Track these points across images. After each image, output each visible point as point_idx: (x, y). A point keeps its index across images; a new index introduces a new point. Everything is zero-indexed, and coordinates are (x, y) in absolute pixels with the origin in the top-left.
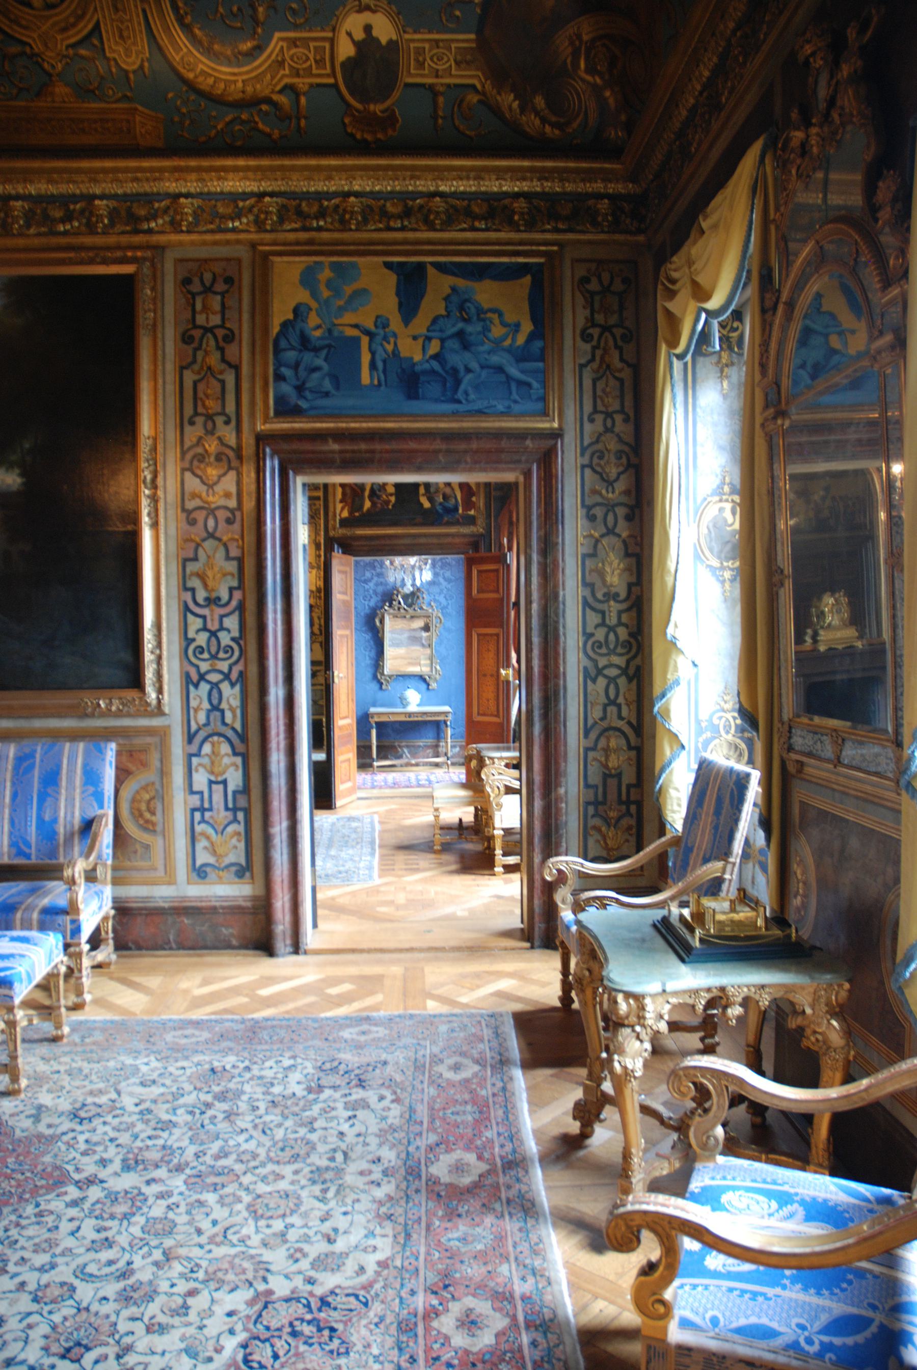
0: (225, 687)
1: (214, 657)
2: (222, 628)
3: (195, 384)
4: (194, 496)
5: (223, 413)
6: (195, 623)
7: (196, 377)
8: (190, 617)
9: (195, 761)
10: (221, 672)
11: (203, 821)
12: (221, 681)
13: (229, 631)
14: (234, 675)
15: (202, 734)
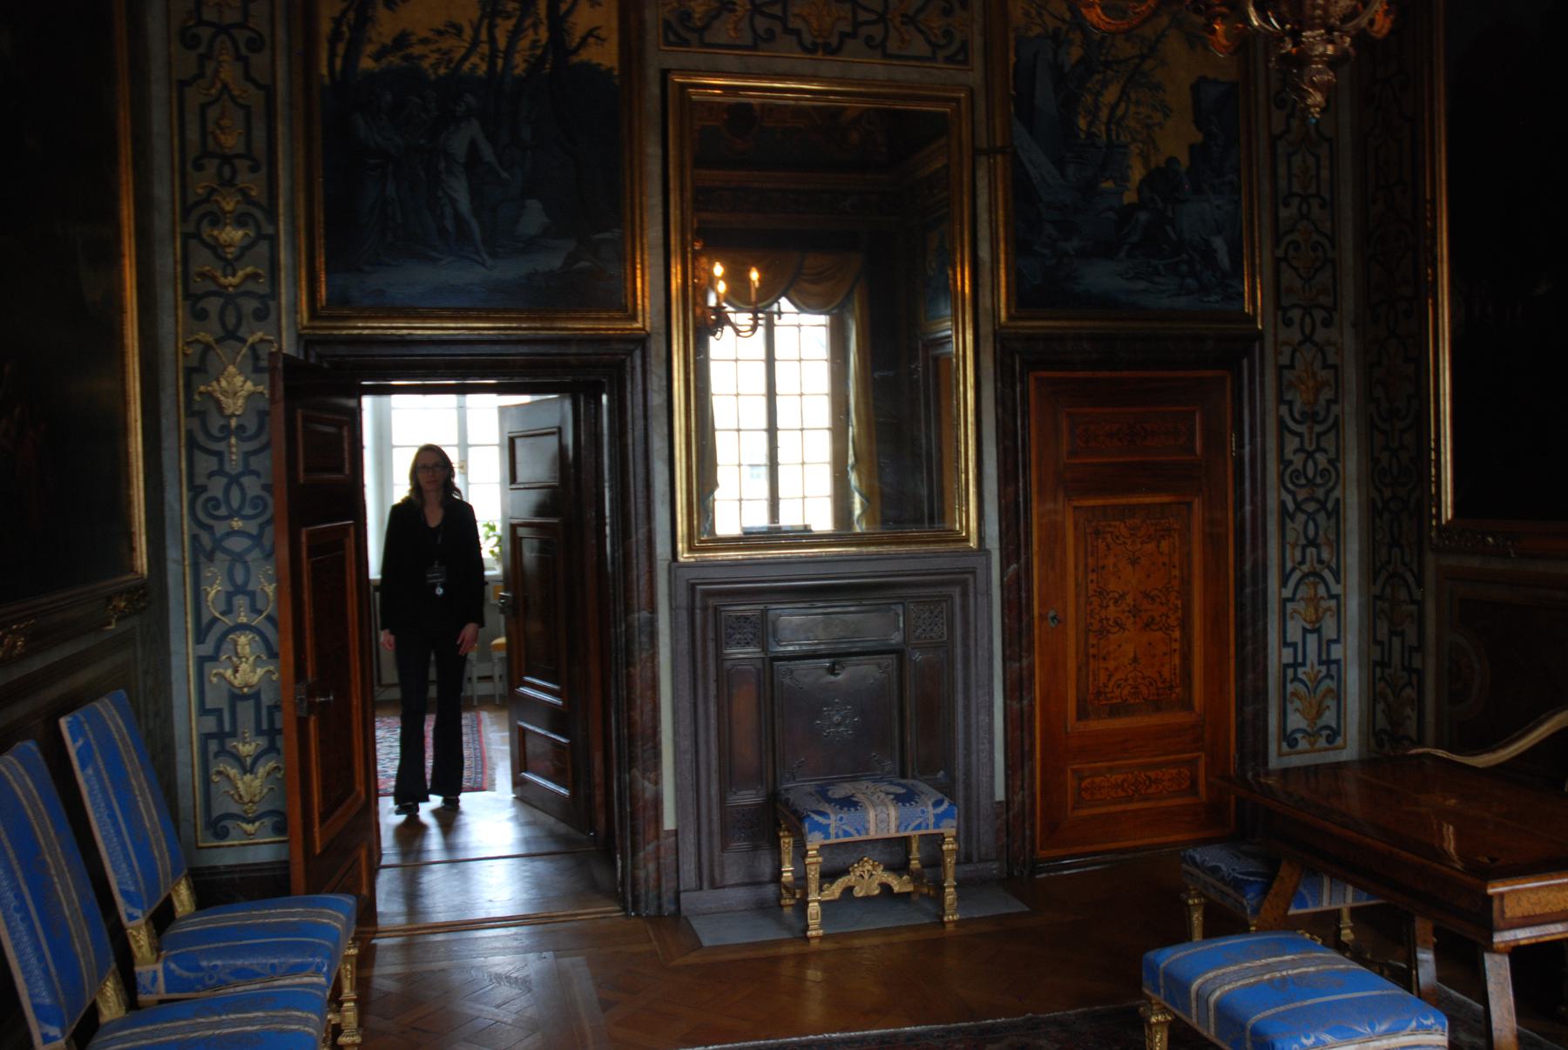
1: (1311, 483)
2: (1319, 449)
6: (1292, 443)
8: (1288, 437)
9: (1290, 606)
10: (1318, 501)
11: (1295, 679)
12: (1318, 511)
13: (1325, 451)
14: (1330, 505)
15: (1297, 575)
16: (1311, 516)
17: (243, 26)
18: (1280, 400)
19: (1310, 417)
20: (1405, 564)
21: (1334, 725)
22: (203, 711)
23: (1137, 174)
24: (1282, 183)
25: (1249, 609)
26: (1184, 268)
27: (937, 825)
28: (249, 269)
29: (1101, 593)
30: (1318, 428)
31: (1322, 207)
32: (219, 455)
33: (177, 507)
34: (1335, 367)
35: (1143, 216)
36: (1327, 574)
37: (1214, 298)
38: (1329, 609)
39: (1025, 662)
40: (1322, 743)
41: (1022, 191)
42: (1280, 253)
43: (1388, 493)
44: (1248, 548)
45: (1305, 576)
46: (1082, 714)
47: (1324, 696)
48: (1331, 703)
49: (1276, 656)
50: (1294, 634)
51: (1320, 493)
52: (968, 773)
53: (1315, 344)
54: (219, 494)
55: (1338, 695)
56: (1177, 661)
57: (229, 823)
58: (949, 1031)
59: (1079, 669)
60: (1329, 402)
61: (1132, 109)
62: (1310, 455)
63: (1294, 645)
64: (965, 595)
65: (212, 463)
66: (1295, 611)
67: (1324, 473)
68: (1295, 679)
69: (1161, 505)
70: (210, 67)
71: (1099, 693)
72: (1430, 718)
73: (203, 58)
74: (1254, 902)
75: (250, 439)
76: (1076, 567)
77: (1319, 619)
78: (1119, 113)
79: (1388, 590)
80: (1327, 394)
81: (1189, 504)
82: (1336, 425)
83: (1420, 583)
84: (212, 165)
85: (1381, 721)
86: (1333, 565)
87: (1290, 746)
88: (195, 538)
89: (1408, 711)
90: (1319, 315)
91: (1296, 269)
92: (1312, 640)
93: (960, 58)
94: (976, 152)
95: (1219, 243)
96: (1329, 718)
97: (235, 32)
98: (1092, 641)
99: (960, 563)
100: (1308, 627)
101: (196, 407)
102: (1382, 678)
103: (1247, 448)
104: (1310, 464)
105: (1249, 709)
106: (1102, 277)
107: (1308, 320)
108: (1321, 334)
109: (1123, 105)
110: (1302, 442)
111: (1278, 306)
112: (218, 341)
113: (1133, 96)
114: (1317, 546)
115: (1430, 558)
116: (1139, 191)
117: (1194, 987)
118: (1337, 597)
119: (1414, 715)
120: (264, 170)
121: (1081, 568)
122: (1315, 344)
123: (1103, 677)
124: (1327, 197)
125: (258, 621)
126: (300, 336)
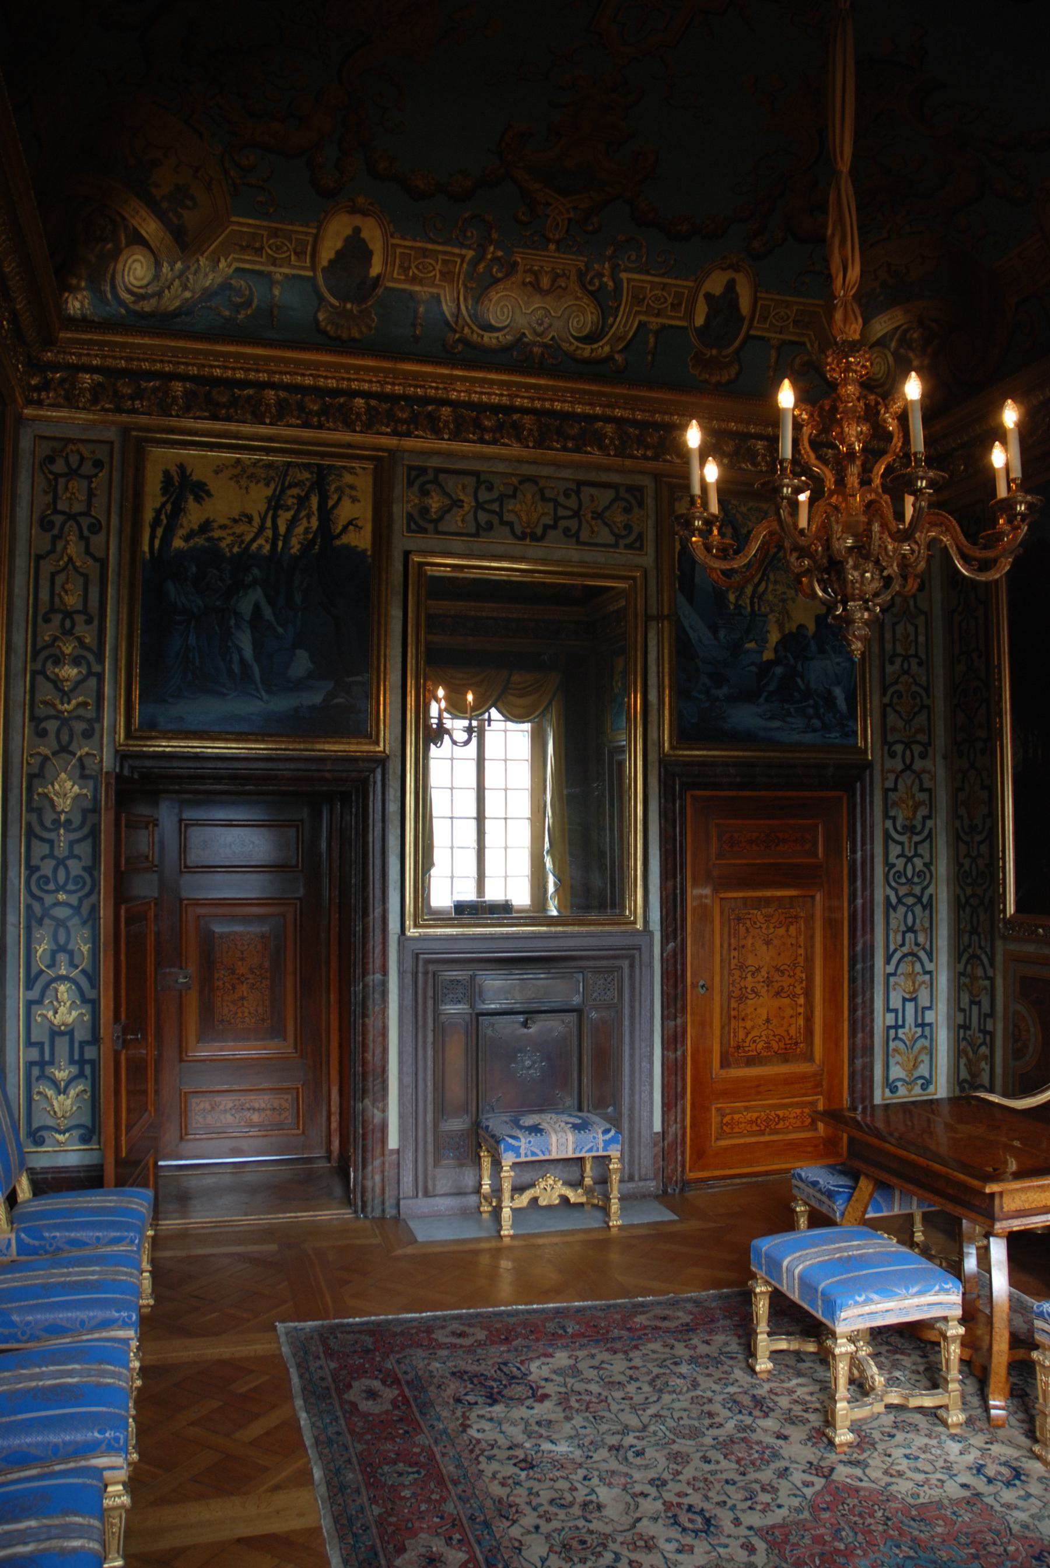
1: (909, 881)
2: (916, 855)
3: (894, 625)
4: (894, 729)
6: (895, 850)
9: (892, 980)
10: (915, 896)
11: (896, 1038)
13: (922, 857)
15: (898, 956)
16: (910, 908)
17: (87, 514)
18: (886, 816)
19: (910, 829)
20: (980, 947)
21: (927, 1076)
22: (29, 1044)
23: (774, 637)
24: (888, 646)
25: (860, 982)
26: (811, 711)
27: (605, 1149)
28: (81, 699)
29: (741, 967)
30: (916, 839)
31: (920, 664)
32: (51, 842)
33: (16, 882)
34: (929, 790)
35: (779, 670)
36: (922, 954)
37: (833, 735)
38: (924, 982)
39: (679, 1021)
41: (683, 650)
42: (886, 700)
43: (969, 891)
44: (859, 933)
45: (905, 956)
46: (725, 1064)
47: (920, 1052)
48: (925, 1058)
49: (881, 1020)
50: (896, 1002)
51: (917, 890)
52: (632, 1109)
53: (914, 772)
54: (50, 875)
55: (931, 1052)
56: (801, 1021)
57: (44, 1133)
58: (609, 1306)
59: (723, 1028)
60: (925, 818)
61: (771, 587)
62: (909, 859)
63: (896, 1011)
64: (632, 966)
65: (45, 849)
66: (896, 984)
67: (920, 874)
68: (896, 1038)
69: (791, 897)
70: (60, 546)
71: (738, 1047)
72: (999, 1070)
73: (55, 539)
74: (842, 1208)
75: (75, 830)
76: (722, 946)
77: (915, 991)
78: (761, 589)
79: (969, 967)
80: (923, 811)
81: (813, 897)
82: (930, 836)
83: (992, 965)
84: (56, 619)
85: (964, 1074)
87: (892, 1092)
88: (29, 907)
89: (983, 1064)
90: (917, 749)
92: (910, 1007)
93: (637, 545)
94: (648, 618)
95: (838, 692)
96: (923, 1070)
97: (81, 519)
98: (734, 1005)
99: (628, 941)
100: (907, 996)
101: (35, 805)
102: (964, 1039)
103: (859, 854)
104: (909, 866)
105: (859, 1062)
106: (745, 717)
107: (908, 753)
108: (918, 765)
109: (763, 584)
111: (885, 742)
112: (54, 754)
113: (772, 577)
114: (915, 932)
115: (999, 944)
116: (776, 650)
117: (785, 1263)
118: (930, 973)
119: (987, 1068)
120: (96, 622)
121: (726, 946)
122: (914, 772)
123: (741, 1034)
124: (924, 657)
125: (74, 973)
126: (117, 752)
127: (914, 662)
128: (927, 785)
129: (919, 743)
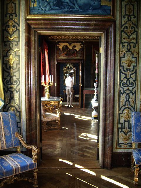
0: (131, 95)
1: (128, 86)
2: (131, 78)
5: (133, 15)
6: (123, 76)
7: (126, 4)
10: (130, 90)
11: (122, 131)
30: (130, 73)
34: (136, 58)
40: (128, 147)
42: (122, 29)
51: (131, 89)
63: (122, 124)
67: (132, 84)
80: (134, 64)
82: (136, 72)
86: (134, 106)
91: (126, 33)
108: (132, 50)
110: (126, 76)
127: (132, 16)
128: (135, 55)
129: (133, 43)
